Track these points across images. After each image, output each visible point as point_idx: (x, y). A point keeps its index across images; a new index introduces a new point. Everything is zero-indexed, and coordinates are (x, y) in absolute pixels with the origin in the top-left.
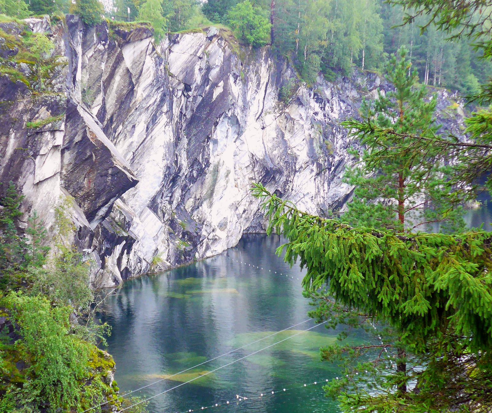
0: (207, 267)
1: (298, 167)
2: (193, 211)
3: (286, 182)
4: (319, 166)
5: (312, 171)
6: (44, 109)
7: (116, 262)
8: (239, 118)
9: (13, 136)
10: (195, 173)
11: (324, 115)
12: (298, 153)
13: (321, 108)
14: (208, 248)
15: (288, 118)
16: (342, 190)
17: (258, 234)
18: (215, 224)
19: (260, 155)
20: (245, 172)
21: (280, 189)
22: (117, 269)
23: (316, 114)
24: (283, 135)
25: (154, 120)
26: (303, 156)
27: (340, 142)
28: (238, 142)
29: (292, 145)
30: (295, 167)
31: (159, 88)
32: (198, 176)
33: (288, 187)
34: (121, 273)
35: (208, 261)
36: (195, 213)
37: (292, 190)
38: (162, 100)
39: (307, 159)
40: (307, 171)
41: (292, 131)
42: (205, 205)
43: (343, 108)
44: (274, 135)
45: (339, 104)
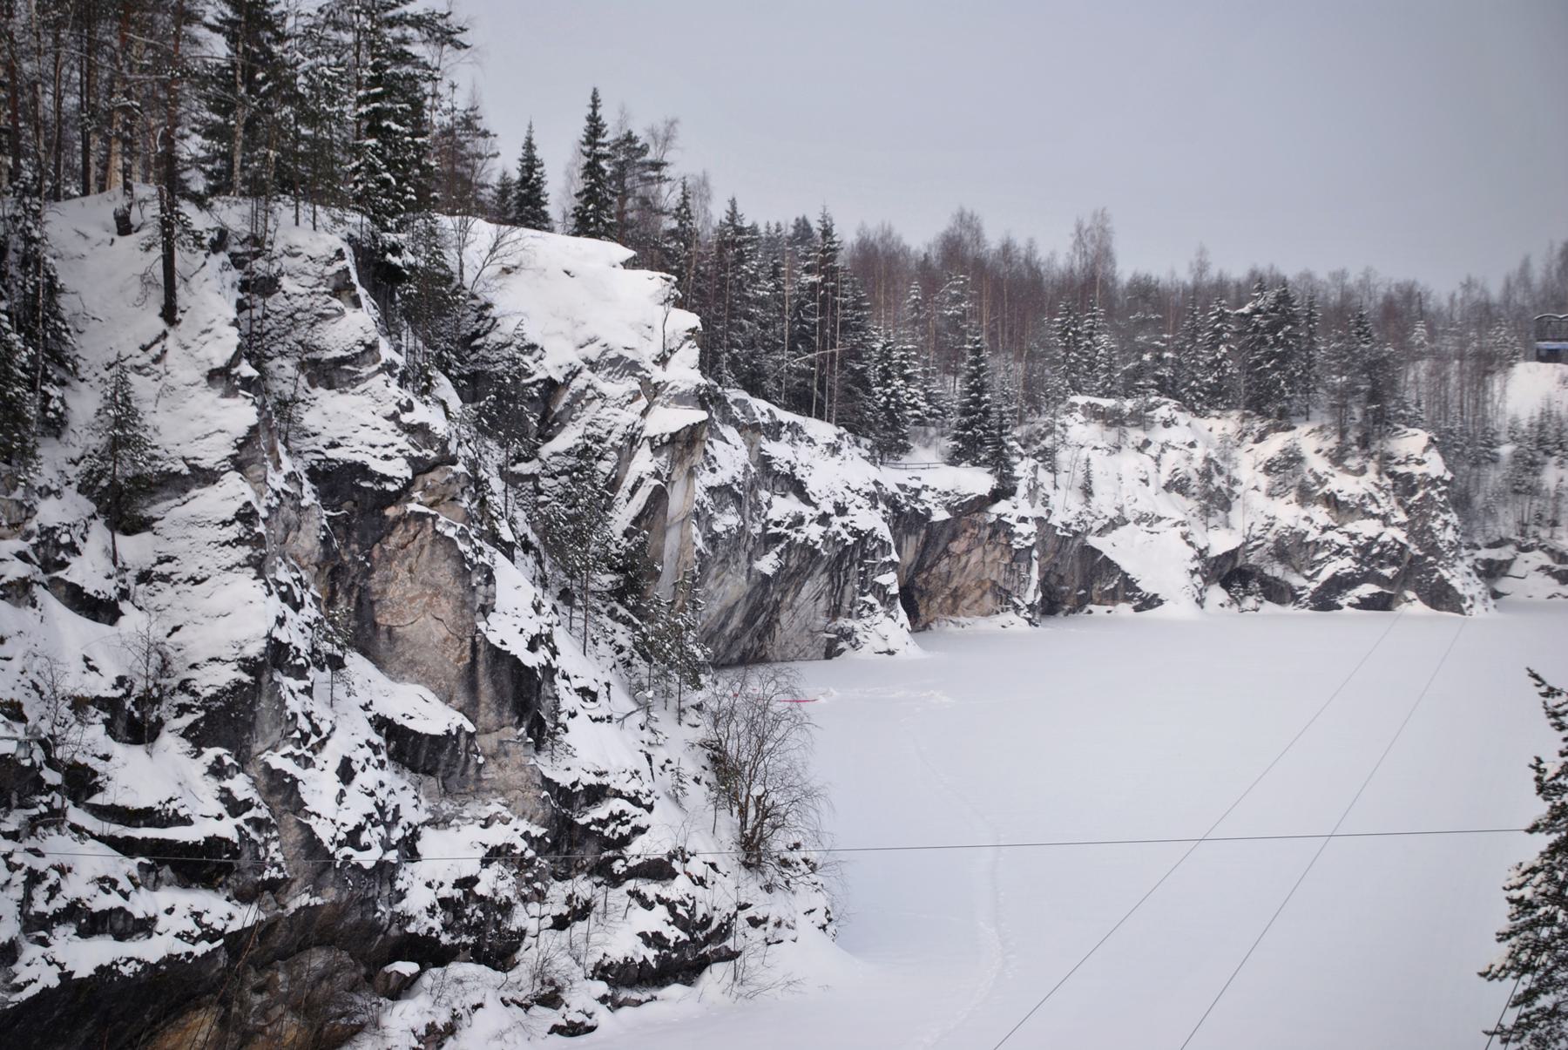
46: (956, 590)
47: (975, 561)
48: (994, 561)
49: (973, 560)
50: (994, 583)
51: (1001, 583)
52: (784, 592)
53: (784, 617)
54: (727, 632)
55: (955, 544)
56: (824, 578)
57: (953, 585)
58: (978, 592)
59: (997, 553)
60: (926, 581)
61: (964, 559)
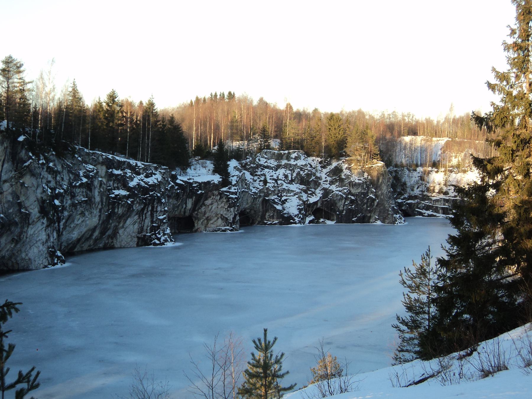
1: (31, 221)
3: (21, 233)
4: (48, 219)
11: (56, 183)
12: (32, 211)
13: (53, 178)
16: (73, 236)
21: (16, 237)
23: (50, 182)
29: (26, 205)
30: (29, 221)
33: (22, 236)
37: (27, 238)
39: (38, 215)
40: (39, 224)
43: (72, 178)
44: (10, 198)
45: (69, 175)
46: (208, 217)
47: (215, 207)
48: (222, 207)
49: (214, 207)
50: (222, 215)
51: (224, 215)
52: (119, 223)
53: (121, 231)
54: (94, 237)
55: (207, 201)
56: (136, 217)
57: (207, 216)
58: (216, 218)
59: (223, 205)
60: (197, 214)
61: (210, 207)
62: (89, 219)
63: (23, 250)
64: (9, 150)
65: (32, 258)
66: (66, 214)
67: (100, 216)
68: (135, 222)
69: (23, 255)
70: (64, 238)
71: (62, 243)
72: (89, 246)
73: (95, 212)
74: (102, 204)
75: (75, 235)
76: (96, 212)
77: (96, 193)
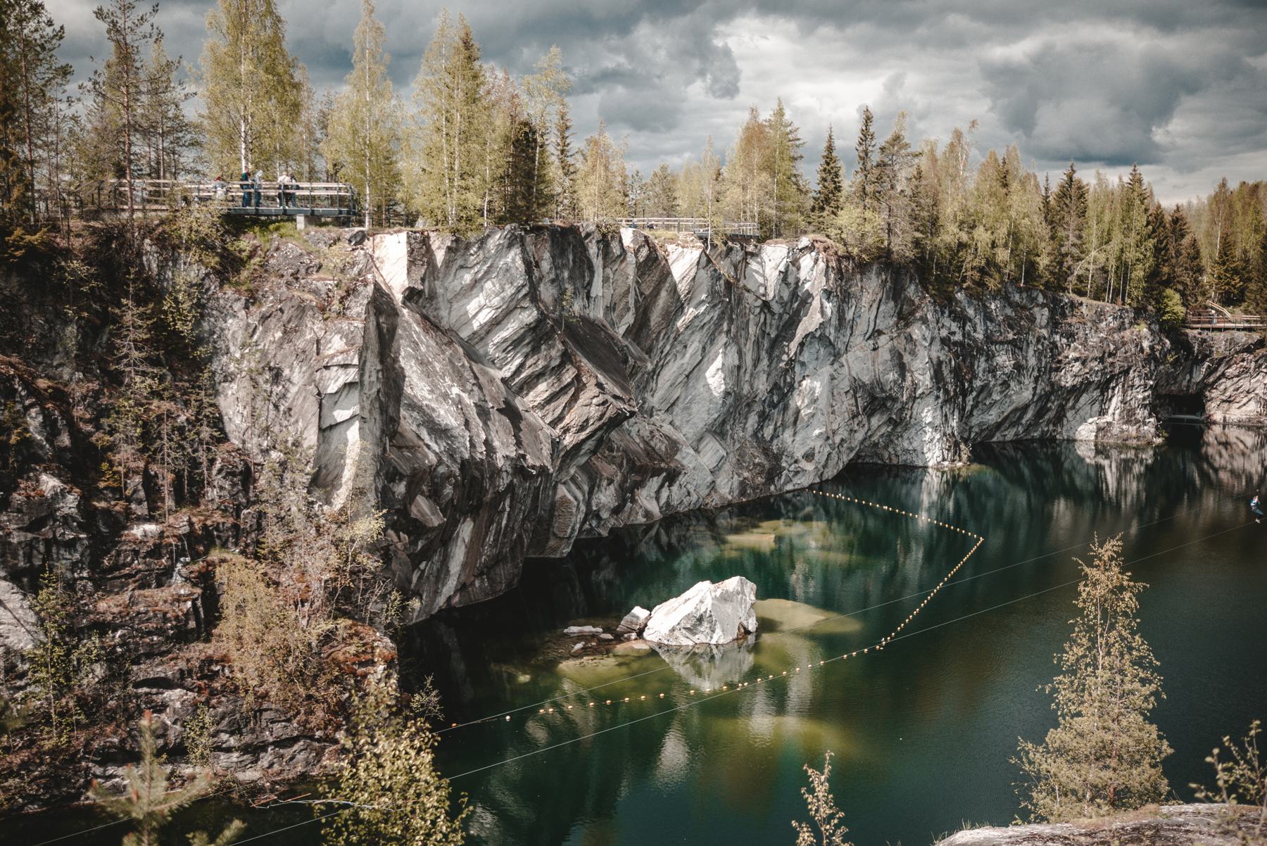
0: (787, 502)
2: (772, 439)
3: (903, 409)
5: (938, 397)
6: (337, 337)
7: (653, 495)
8: (832, 338)
9: (297, 370)
10: (775, 399)
11: (964, 336)
14: (786, 483)
15: (909, 339)
17: (876, 464)
18: (798, 455)
19: (866, 379)
20: (844, 398)
22: (655, 502)
23: (954, 333)
24: (900, 356)
25: (712, 339)
26: (925, 380)
27: (983, 365)
28: (836, 366)
31: (715, 306)
32: (779, 402)
34: (661, 508)
35: (789, 496)
36: (775, 442)
38: (721, 318)
40: (931, 399)
41: (913, 353)
42: (787, 435)
44: (888, 356)
45: (985, 324)
53: (1070, 414)
54: (1024, 421)
62: (1016, 393)
63: (905, 436)
64: (889, 284)
65: (919, 449)
66: (978, 383)
67: (1035, 389)
68: (1096, 400)
69: (906, 444)
70: (974, 421)
71: (971, 428)
72: (1016, 434)
73: (1027, 382)
74: (1039, 371)
75: (992, 417)
76: (1028, 381)
77: (1031, 352)
